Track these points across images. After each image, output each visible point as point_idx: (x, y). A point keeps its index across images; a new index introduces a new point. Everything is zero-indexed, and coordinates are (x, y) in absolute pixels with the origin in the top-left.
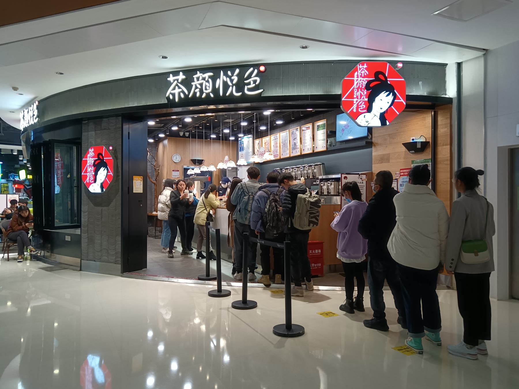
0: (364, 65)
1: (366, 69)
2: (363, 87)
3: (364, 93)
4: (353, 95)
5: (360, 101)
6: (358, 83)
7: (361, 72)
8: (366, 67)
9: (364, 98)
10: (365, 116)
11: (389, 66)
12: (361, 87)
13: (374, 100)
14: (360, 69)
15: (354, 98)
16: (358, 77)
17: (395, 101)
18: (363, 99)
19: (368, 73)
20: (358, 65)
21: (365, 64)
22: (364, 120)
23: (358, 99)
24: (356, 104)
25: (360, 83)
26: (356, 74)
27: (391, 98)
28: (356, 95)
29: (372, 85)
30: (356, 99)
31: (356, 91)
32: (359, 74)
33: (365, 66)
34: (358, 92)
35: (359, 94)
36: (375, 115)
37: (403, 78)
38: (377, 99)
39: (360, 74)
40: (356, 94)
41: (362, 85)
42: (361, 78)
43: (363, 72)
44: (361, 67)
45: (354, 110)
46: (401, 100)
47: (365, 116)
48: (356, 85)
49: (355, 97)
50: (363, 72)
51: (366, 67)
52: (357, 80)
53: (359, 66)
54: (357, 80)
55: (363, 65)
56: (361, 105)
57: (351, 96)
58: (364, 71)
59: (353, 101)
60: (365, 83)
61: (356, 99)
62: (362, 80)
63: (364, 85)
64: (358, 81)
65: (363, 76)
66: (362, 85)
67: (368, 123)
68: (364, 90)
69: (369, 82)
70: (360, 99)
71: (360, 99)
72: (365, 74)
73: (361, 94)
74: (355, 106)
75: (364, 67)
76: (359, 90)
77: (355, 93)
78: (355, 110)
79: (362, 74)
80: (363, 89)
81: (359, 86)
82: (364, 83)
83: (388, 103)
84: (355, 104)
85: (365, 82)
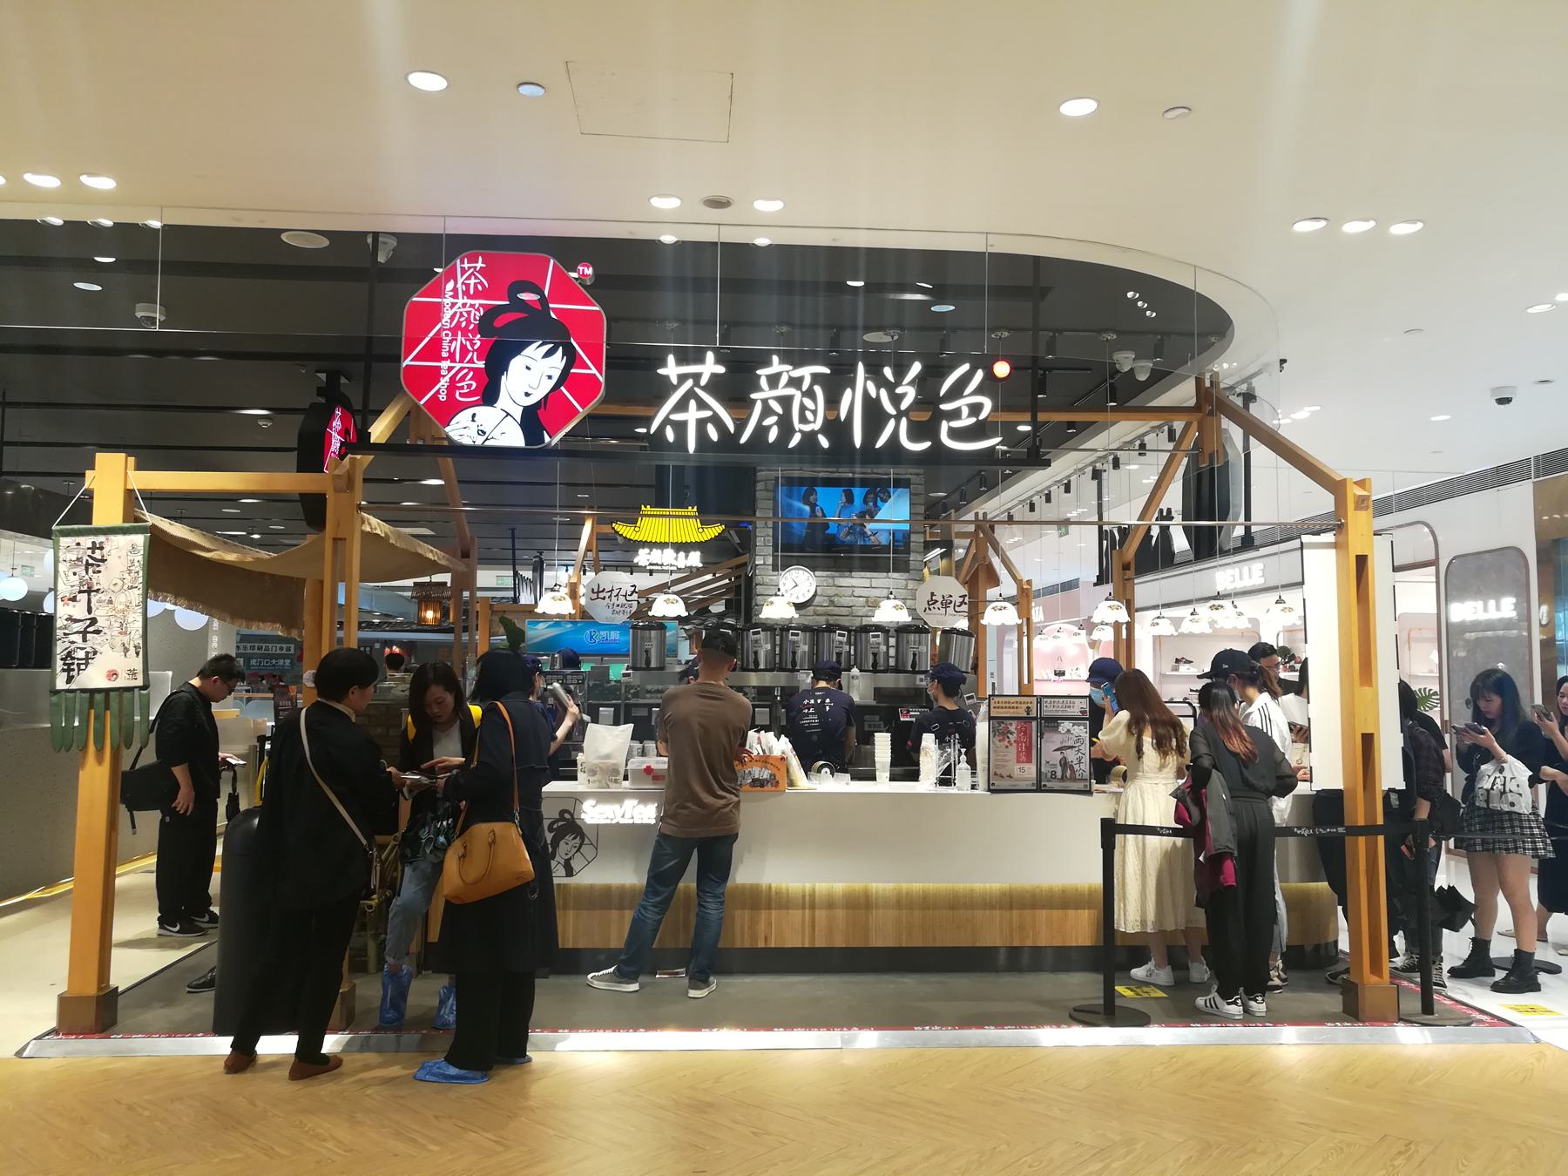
0: (477, 262)
1: (482, 271)
2: (472, 327)
3: (473, 345)
4: (440, 348)
5: (462, 369)
6: (456, 313)
7: (467, 282)
8: (484, 266)
9: (472, 357)
10: (474, 415)
11: (554, 264)
12: (464, 324)
13: (504, 368)
14: (464, 271)
15: (441, 359)
16: (455, 296)
17: (573, 371)
18: (471, 361)
19: (485, 283)
20: (458, 261)
21: (480, 259)
22: (473, 427)
23: (453, 361)
24: (447, 378)
25: (461, 313)
26: (450, 286)
27: (558, 361)
28: (449, 351)
29: (499, 322)
30: (449, 361)
31: (449, 338)
32: (459, 285)
33: (480, 265)
34: (454, 342)
35: (456, 346)
36: (508, 414)
37: (595, 303)
38: (517, 364)
39: (464, 289)
40: (450, 347)
41: (468, 321)
42: (466, 300)
43: (472, 281)
44: (466, 265)
45: (440, 397)
46: (590, 369)
47: (474, 415)
48: (449, 321)
49: (444, 354)
50: (472, 281)
51: (484, 266)
52: (453, 305)
53: (462, 262)
54: (453, 305)
55: (473, 260)
56: (463, 379)
57: (433, 350)
58: (476, 278)
59: (439, 368)
60: (477, 313)
61: (449, 361)
62: (468, 305)
63: (475, 319)
64: (455, 309)
65: (472, 292)
66: (468, 321)
67: (485, 437)
68: (474, 336)
69: (491, 313)
70: (461, 361)
71: (461, 361)
72: (480, 288)
73: (463, 347)
74: (444, 383)
75: (475, 268)
76: (459, 333)
77: (445, 345)
78: (443, 397)
79: (468, 286)
80: (470, 331)
81: (459, 323)
82: (475, 315)
83: (550, 377)
84: (444, 376)
85: (478, 310)
